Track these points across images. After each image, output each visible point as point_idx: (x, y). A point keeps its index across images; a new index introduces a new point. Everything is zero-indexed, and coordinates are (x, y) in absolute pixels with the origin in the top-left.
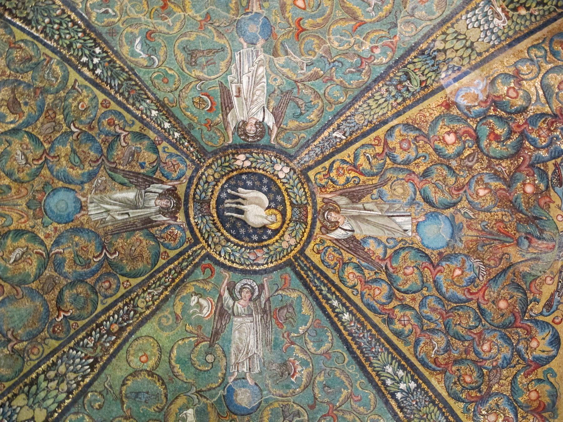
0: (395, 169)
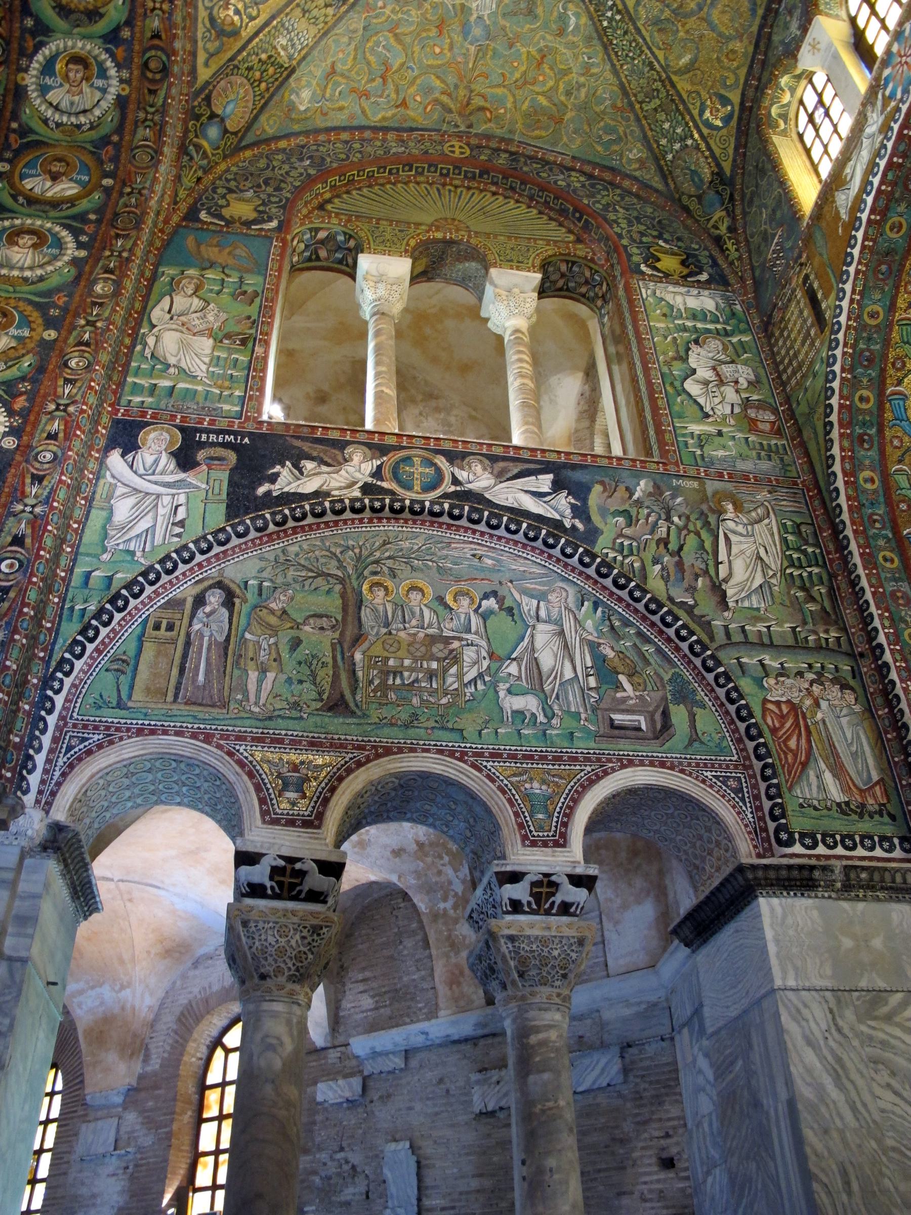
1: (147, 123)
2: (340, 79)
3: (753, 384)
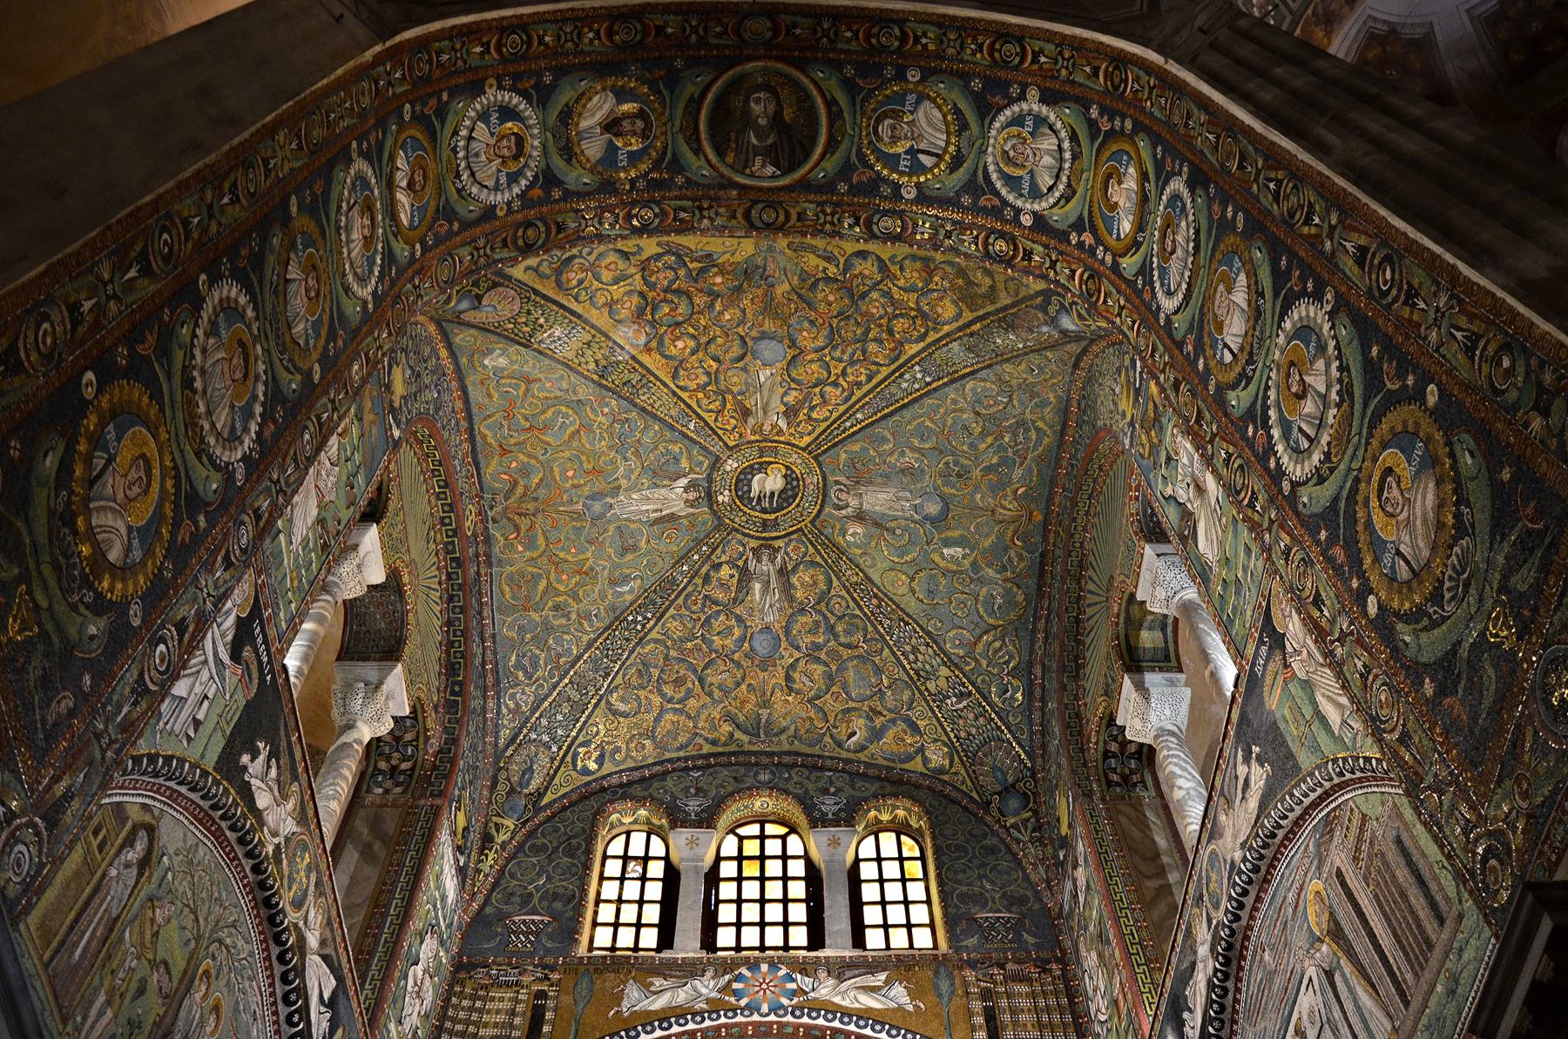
0: (717, 382)
1: (475, 253)
2: (523, 387)
3: (427, 1015)
